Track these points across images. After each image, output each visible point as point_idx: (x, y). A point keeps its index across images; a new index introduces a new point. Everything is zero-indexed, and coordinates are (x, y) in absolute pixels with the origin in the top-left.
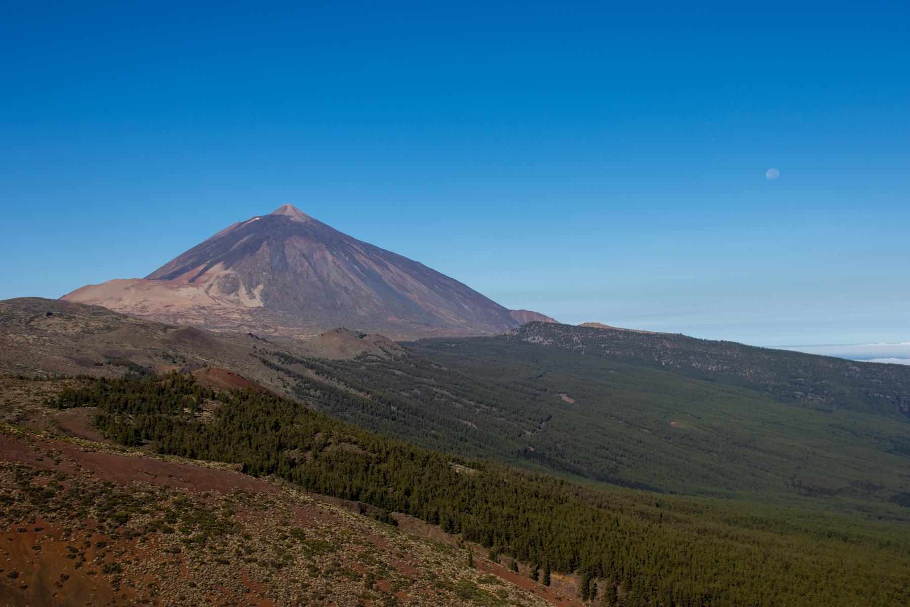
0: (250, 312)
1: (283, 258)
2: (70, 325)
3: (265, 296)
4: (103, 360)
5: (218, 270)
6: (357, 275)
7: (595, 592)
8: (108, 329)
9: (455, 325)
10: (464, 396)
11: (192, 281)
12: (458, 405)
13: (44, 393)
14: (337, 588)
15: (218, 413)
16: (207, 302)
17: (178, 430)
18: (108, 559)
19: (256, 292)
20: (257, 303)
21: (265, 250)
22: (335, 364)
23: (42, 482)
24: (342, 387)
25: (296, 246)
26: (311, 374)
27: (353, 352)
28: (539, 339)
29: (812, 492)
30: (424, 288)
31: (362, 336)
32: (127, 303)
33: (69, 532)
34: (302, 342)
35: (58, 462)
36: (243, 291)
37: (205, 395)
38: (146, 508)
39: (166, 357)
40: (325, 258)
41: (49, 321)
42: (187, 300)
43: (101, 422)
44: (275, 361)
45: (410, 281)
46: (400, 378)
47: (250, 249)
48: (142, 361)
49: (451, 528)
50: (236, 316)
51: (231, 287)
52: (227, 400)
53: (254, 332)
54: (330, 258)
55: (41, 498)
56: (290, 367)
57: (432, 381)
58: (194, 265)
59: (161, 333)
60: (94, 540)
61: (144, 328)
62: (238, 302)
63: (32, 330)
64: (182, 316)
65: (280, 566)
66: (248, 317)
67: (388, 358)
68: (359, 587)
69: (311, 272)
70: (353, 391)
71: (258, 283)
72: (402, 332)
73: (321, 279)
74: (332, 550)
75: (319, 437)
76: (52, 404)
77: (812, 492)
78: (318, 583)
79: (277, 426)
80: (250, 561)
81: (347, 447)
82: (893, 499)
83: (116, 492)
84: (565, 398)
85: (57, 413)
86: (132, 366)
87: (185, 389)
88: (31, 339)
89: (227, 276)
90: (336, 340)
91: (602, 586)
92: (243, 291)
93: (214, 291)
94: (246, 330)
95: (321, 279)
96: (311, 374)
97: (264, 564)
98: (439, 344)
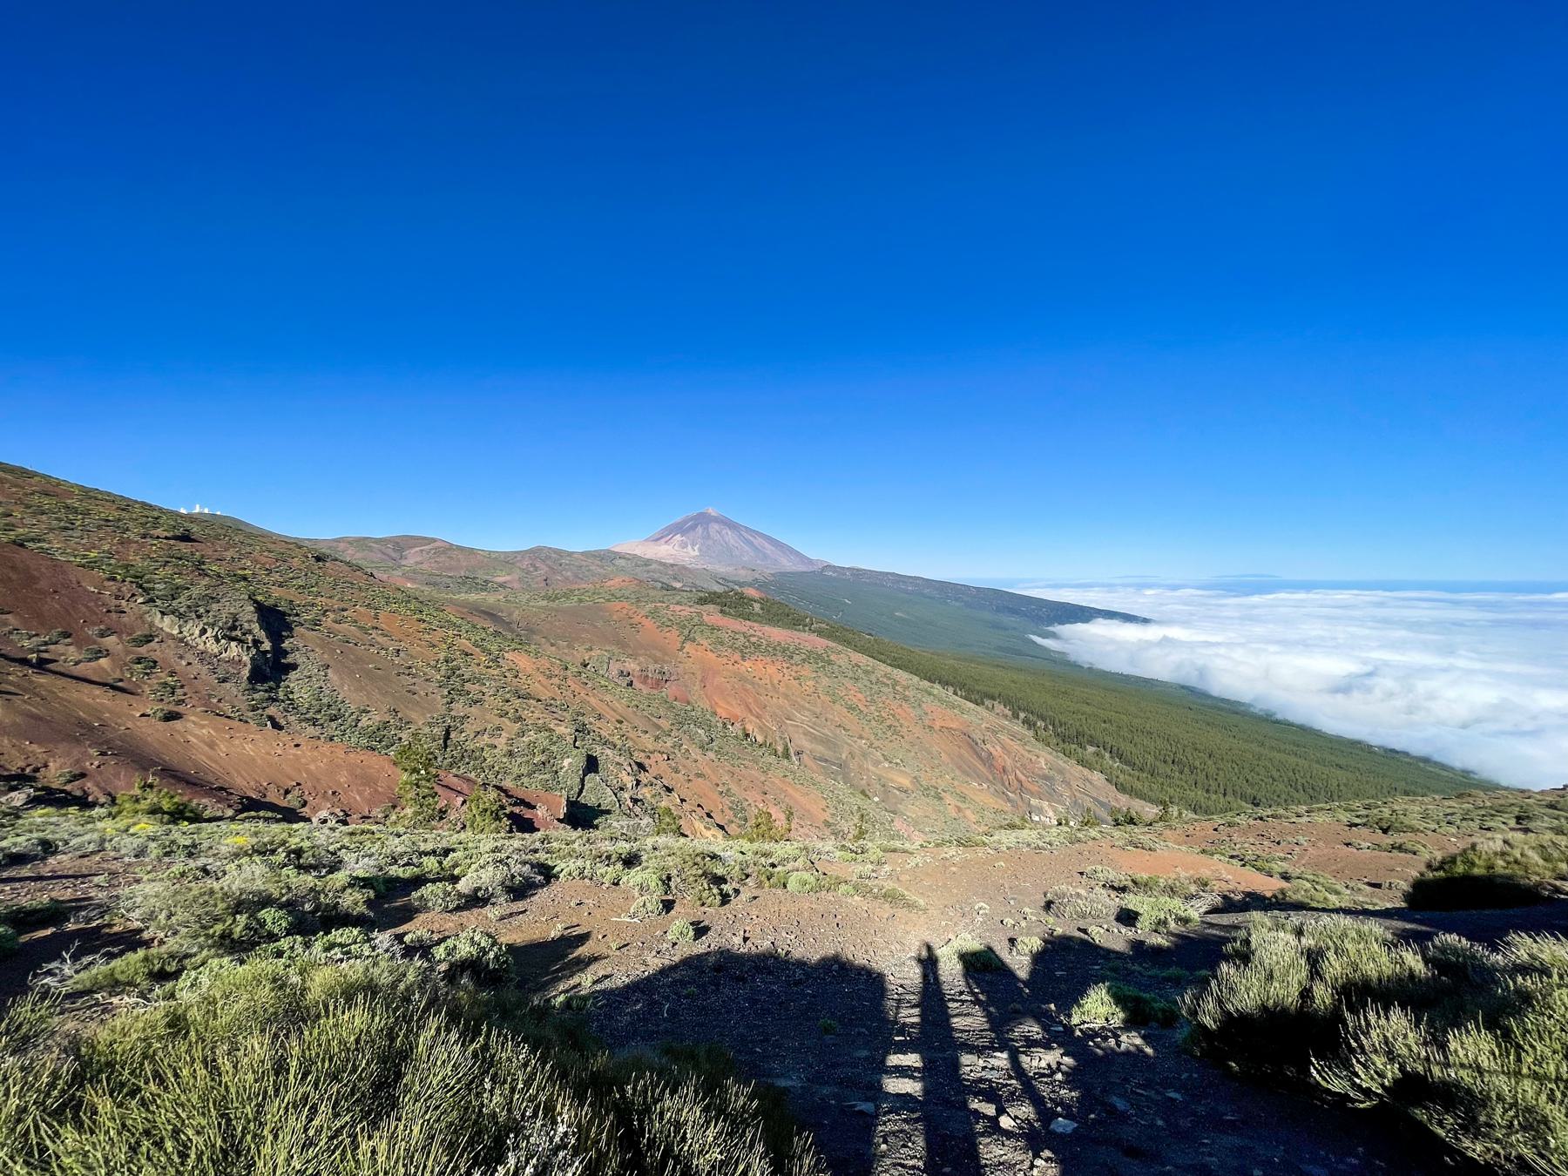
9: (788, 565)
32: (638, 552)
42: (667, 551)
47: (693, 528)
51: (684, 545)
55: (757, 646)
72: (767, 570)
90: (743, 572)
98: (783, 574)
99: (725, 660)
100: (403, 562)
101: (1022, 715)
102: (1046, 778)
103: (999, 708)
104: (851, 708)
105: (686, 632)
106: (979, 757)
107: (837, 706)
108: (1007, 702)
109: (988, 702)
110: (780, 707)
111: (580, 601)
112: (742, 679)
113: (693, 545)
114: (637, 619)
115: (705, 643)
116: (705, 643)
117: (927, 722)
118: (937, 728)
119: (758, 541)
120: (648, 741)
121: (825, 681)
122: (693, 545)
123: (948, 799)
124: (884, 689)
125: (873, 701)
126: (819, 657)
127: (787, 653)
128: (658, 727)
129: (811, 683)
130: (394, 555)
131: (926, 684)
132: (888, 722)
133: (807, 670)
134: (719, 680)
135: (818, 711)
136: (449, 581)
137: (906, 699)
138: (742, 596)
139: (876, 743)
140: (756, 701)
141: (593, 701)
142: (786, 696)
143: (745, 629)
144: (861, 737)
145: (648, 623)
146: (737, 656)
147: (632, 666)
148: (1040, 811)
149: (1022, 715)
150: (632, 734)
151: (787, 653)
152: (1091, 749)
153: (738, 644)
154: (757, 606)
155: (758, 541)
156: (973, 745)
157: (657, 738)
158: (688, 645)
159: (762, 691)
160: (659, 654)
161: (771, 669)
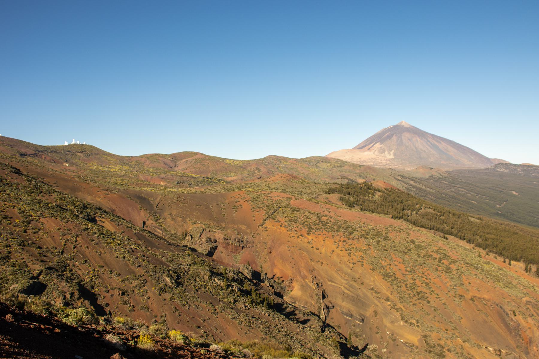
0: (389, 160)
3: (395, 154)
4: (340, 177)
5: (378, 145)
6: (429, 146)
7: (530, 270)
8: (341, 166)
9: (468, 164)
10: (471, 192)
11: (369, 149)
12: (469, 195)
13: (323, 189)
15: (381, 197)
16: (373, 156)
17: (367, 202)
18: (347, 246)
19: (392, 153)
20: (392, 157)
21: (395, 138)
22: (421, 179)
23: (323, 219)
24: (424, 187)
25: (406, 136)
26: (412, 182)
27: (427, 176)
28: (503, 170)
30: (455, 151)
31: (431, 169)
32: (346, 158)
33: (333, 236)
34: (409, 171)
35: (329, 212)
36: (386, 152)
37: (375, 190)
39: (361, 176)
40: (417, 140)
41: (322, 164)
42: (368, 157)
43: (341, 199)
44: (399, 178)
45: (450, 148)
46: (446, 184)
47: (389, 137)
48: (353, 178)
49: (469, 242)
51: (382, 151)
52: (384, 192)
53: (391, 167)
55: (325, 224)
56: (405, 180)
57: (459, 186)
58: (370, 144)
59: (359, 168)
60: (342, 239)
61: (353, 165)
62: (385, 157)
63: (317, 167)
65: (406, 253)
66: (388, 162)
67: (441, 177)
68: (436, 263)
70: (428, 189)
71: (392, 150)
73: (416, 148)
75: (417, 206)
78: (421, 260)
79: (402, 202)
80: (395, 250)
81: (428, 210)
83: (348, 224)
84: (514, 193)
85: (328, 195)
86: (349, 179)
87: (368, 188)
88: (317, 170)
89: (381, 148)
90: (421, 170)
91: (534, 268)
92: (386, 152)
93: (376, 153)
94: (388, 167)
95: (416, 148)
96: (412, 182)
97: (400, 252)
98: (461, 172)
99: (293, 234)
100: (176, 169)
104: (386, 276)
105: (271, 212)
106: (507, 326)
113: (390, 150)
114: (241, 202)
116: (283, 220)
118: (468, 296)
119: (442, 146)
121: (374, 252)
122: (390, 150)
129: (361, 254)
130: (171, 164)
133: (361, 244)
134: (284, 248)
136: (192, 180)
137: (448, 270)
139: (400, 306)
144: (388, 299)
146: (304, 231)
147: (219, 236)
153: (310, 221)
156: (502, 316)
158: (269, 224)
160: (243, 227)
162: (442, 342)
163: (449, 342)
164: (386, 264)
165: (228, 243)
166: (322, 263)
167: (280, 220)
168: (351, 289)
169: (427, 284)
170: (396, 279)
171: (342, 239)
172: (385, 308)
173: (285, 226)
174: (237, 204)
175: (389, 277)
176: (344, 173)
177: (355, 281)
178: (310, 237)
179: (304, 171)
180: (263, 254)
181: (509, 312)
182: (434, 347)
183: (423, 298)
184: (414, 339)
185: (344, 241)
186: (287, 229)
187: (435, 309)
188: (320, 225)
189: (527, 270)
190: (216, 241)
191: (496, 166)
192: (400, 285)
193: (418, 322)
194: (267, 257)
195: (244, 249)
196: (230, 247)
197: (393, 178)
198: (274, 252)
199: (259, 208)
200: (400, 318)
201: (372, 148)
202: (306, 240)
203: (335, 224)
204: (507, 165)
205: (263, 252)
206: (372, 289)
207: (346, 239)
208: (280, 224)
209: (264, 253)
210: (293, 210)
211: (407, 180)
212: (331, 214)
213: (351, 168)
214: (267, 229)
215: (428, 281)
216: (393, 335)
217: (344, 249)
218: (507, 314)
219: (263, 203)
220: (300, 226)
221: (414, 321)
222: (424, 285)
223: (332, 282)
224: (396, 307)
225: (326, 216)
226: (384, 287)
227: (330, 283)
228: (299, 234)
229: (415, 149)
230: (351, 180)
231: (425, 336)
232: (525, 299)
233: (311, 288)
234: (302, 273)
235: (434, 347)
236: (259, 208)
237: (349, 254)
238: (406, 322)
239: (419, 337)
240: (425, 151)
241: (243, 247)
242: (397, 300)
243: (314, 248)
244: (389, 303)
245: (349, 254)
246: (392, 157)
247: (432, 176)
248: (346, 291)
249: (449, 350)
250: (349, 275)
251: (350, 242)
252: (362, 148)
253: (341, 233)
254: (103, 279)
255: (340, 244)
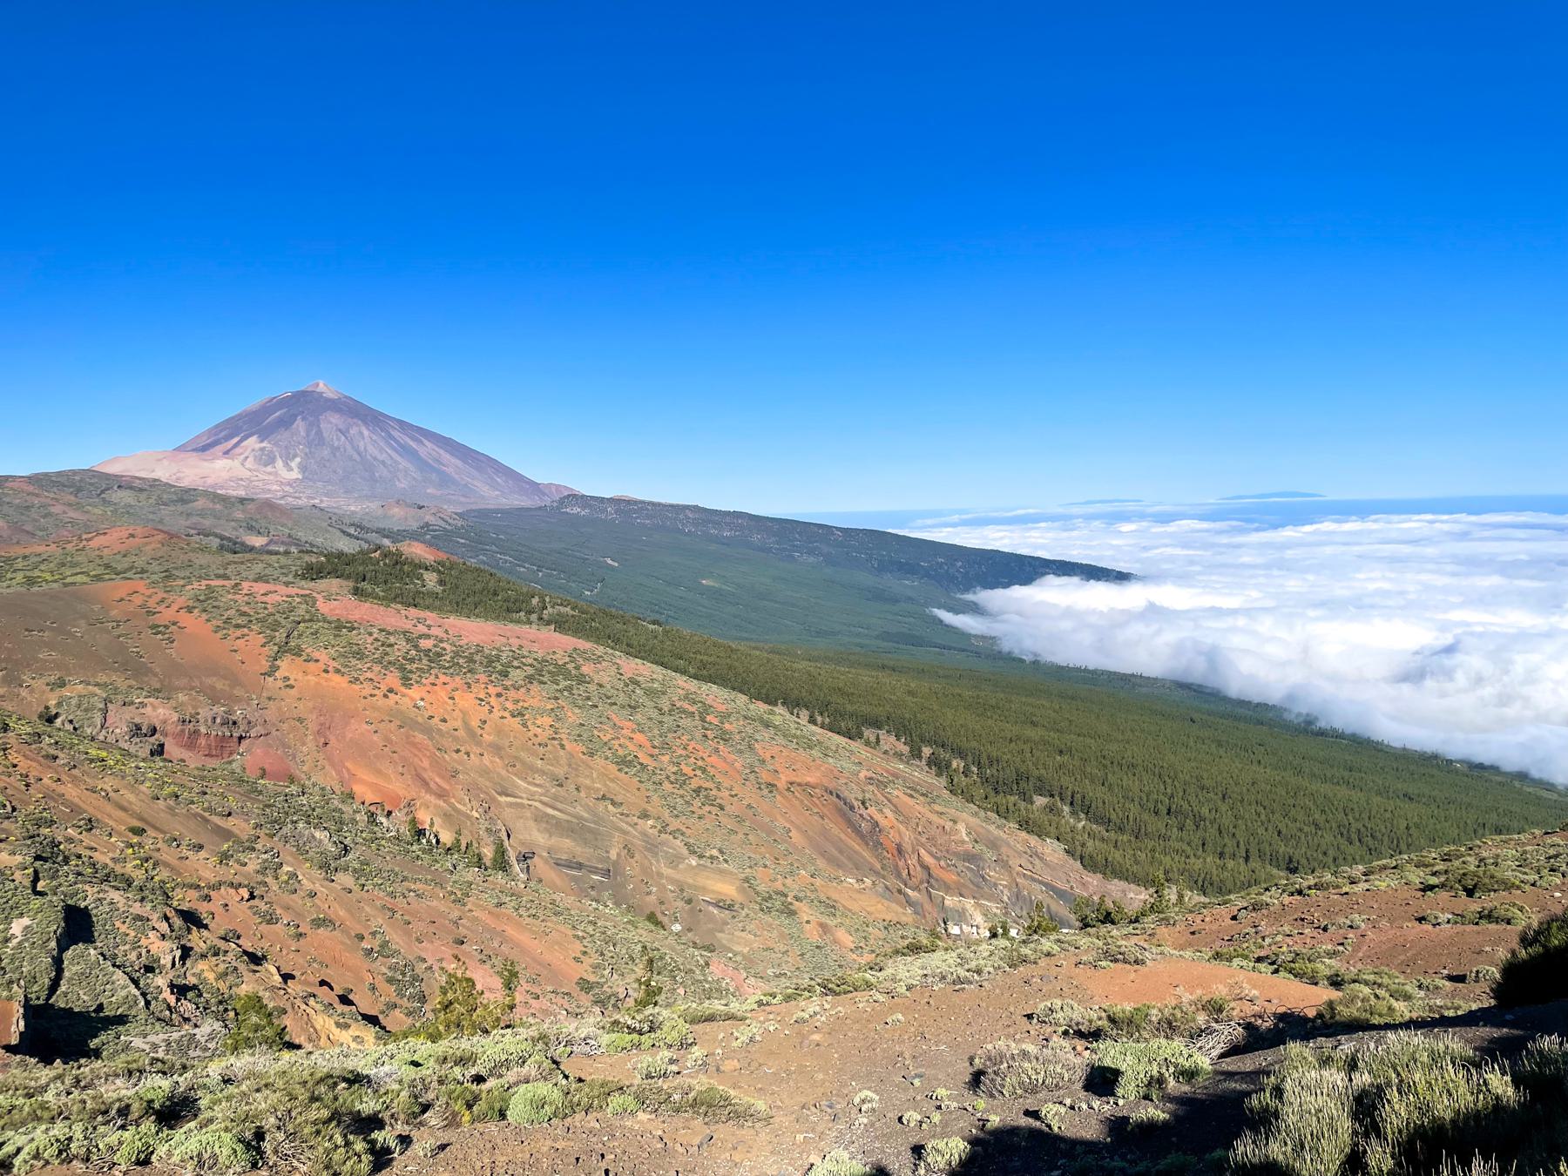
1: (319, 433)
2: (143, 496)
3: (303, 468)
5: (252, 442)
8: (183, 501)
9: (492, 496)
11: (226, 453)
14: (682, 723)
20: (295, 474)
21: (300, 425)
23: (425, 644)
25: (331, 422)
28: (576, 510)
29: (819, 633)
30: (459, 463)
31: (421, 508)
32: (163, 473)
34: (353, 513)
36: (279, 463)
38: (516, 663)
39: (251, 528)
40: (361, 433)
42: (225, 472)
45: (446, 456)
47: (285, 423)
50: (275, 487)
51: (271, 461)
54: (366, 433)
55: (434, 657)
58: (227, 438)
62: (276, 474)
64: (222, 487)
66: (287, 488)
69: (349, 447)
71: (295, 456)
72: (448, 506)
74: (664, 693)
75: (535, 601)
76: (303, 577)
77: (819, 633)
81: (562, 609)
82: (877, 637)
86: (222, 538)
89: (262, 449)
92: (279, 463)
93: (250, 463)
98: (484, 514)
101: (927, 751)
102: (970, 857)
103: (889, 741)
104: (624, 763)
105: (280, 635)
106: (857, 831)
107: (599, 761)
108: (901, 729)
109: (869, 733)
110: (485, 772)
111: (31, 581)
112: (406, 723)
113: (287, 459)
114: (167, 615)
115: (323, 656)
117: (765, 777)
118: (782, 784)
120: (204, 866)
121: (573, 716)
122: (287, 459)
123: (805, 912)
124: (685, 722)
125: (666, 746)
126: (561, 670)
127: (495, 666)
128: (226, 835)
129: (547, 721)
131: (761, 707)
132: (695, 783)
133: (536, 697)
134: (358, 729)
135: (560, 772)
137: (725, 737)
138: (397, 560)
139: (675, 824)
140: (436, 764)
141: (71, 791)
142: (497, 749)
143: (408, 626)
144: (645, 815)
145: (194, 623)
146: (393, 679)
147: (159, 712)
148: (961, 917)
149: (927, 751)
150: (168, 854)
151: (495, 666)
152: (1040, 801)
154: (431, 579)
155: (427, 449)
157: (224, 858)
158: (286, 666)
159: (447, 742)
160: (220, 685)
161: (466, 701)
162: (778, 885)
163: (789, 881)
164: (609, 736)
165: (196, 732)
166: (468, 754)
167: (316, 655)
168: (559, 805)
169: (704, 771)
170: (644, 767)
171: (492, 690)
172: (644, 834)
173: (338, 671)
174: (157, 620)
175: (629, 764)
176: (195, 519)
177: (561, 785)
178: (415, 693)
179: (72, 514)
180: (305, 749)
181: (856, 804)
182: (770, 898)
183: (710, 801)
184: (728, 889)
185: (499, 695)
186: (347, 678)
187: (740, 820)
188: (425, 661)
189: (812, 721)
190: (154, 731)
191: (562, 501)
192: (656, 778)
193: (721, 852)
194: (321, 756)
195: (245, 743)
196: (202, 741)
197: (338, 533)
198: (333, 741)
199: (238, 626)
200: (685, 851)
201: (238, 450)
202: (406, 699)
203: (457, 654)
204: (584, 500)
205: (304, 744)
206: (604, 797)
207: (499, 689)
208: (321, 665)
209: (308, 747)
210: (339, 628)
211: (373, 536)
212: (435, 631)
213: (218, 506)
214: (291, 682)
215: (700, 763)
216: (682, 890)
217: (506, 714)
218: (852, 808)
219: (244, 614)
220: (377, 668)
221: (715, 852)
222: (698, 773)
223: (507, 795)
224: (669, 829)
225: (428, 637)
226: (625, 786)
227: (503, 799)
228: (384, 688)
229: (356, 456)
230: (229, 539)
231: (746, 880)
232: (862, 775)
233: (469, 817)
234: (432, 785)
235: (770, 898)
236: (238, 626)
237: (525, 725)
238: (701, 857)
239: (738, 883)
240: (383, 462)
241: (241, 738)
242: (666, 813)
243: (436, 720)
244: (650, 822)
245: (525, 725)
246: (295, 474)
247: (427, 525)
248: (550, 811)
249: (797, 899)
250: (542, 773)
251: (512, 694)
252: (204, 449)
253: (483, 678)
254: (166, 865)
255: (493, 700)
